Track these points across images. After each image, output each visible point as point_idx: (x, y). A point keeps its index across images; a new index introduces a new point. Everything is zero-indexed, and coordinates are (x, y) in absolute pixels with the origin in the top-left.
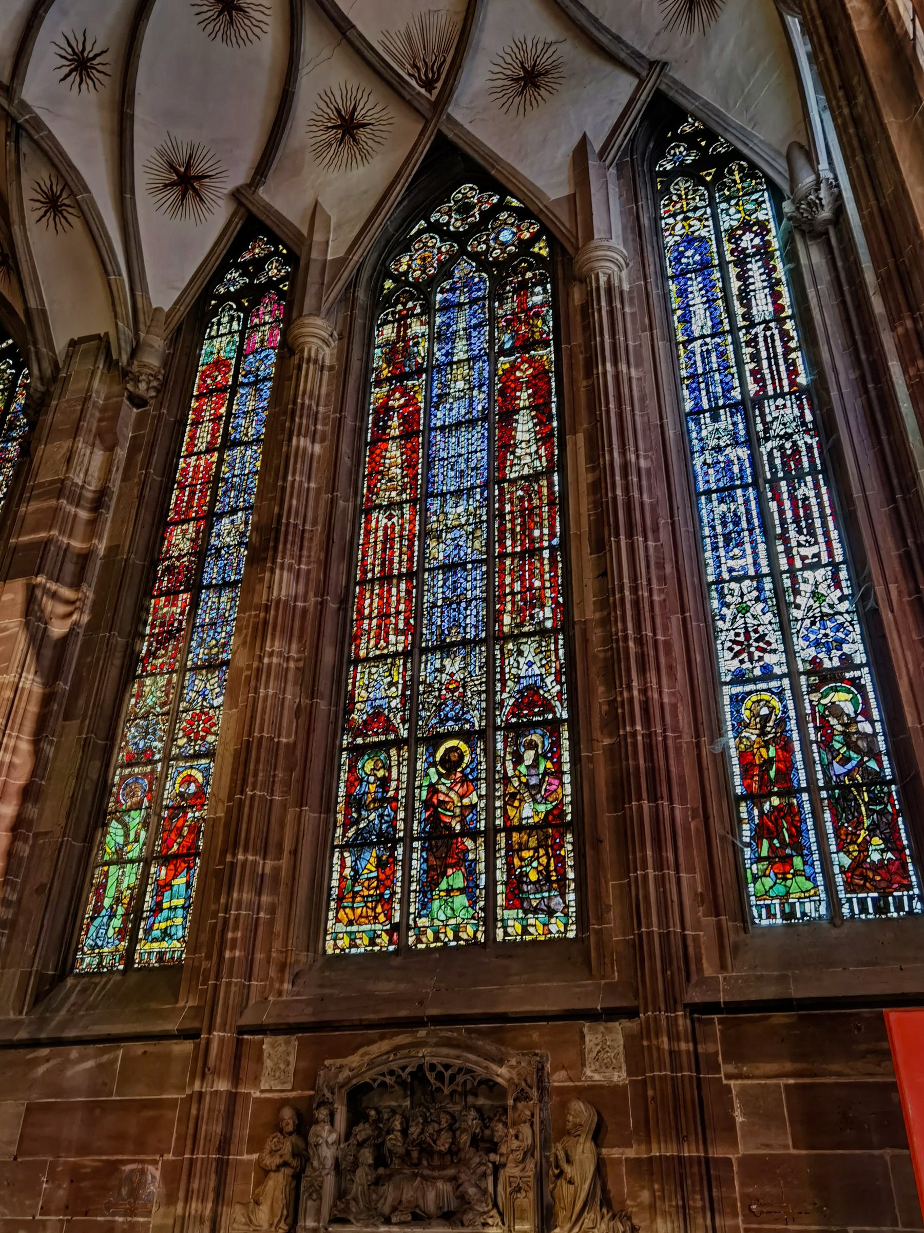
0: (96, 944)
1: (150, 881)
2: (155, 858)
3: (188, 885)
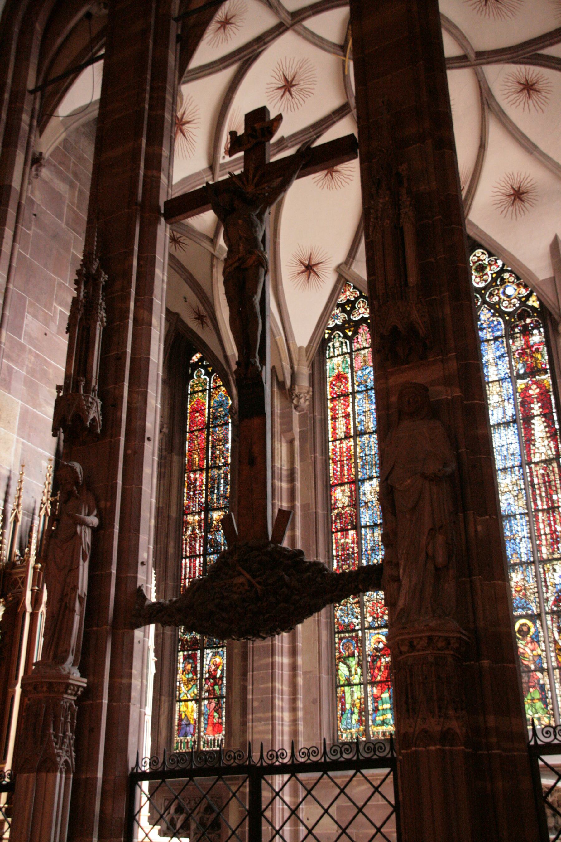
0: (347, 728)
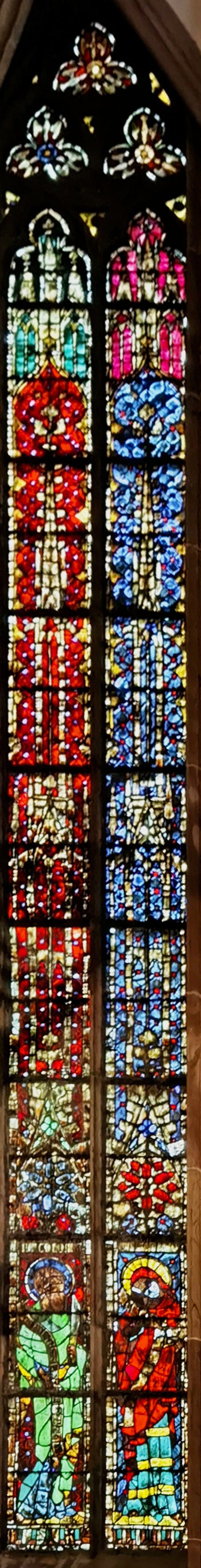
1: (108, 1427)
2: (110, 1393)
3: (175, 1439)
